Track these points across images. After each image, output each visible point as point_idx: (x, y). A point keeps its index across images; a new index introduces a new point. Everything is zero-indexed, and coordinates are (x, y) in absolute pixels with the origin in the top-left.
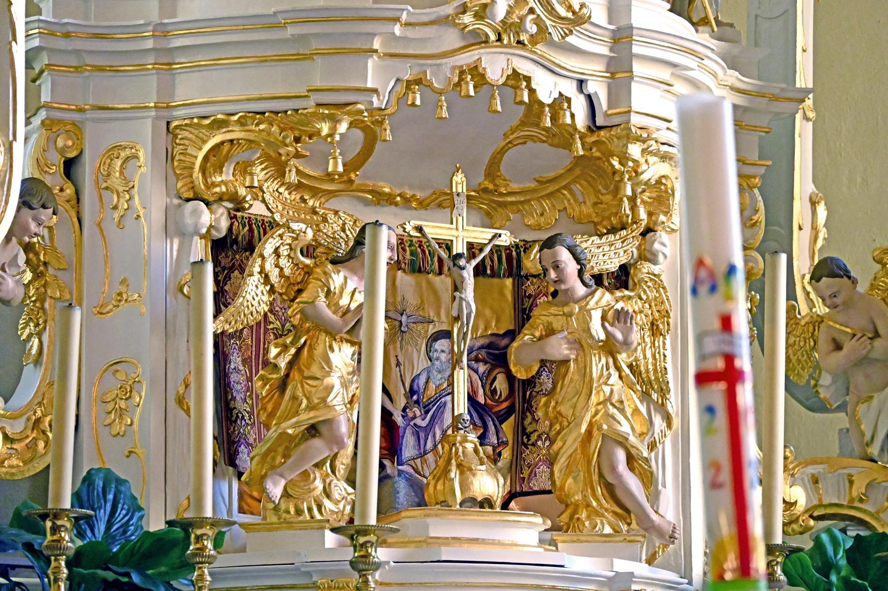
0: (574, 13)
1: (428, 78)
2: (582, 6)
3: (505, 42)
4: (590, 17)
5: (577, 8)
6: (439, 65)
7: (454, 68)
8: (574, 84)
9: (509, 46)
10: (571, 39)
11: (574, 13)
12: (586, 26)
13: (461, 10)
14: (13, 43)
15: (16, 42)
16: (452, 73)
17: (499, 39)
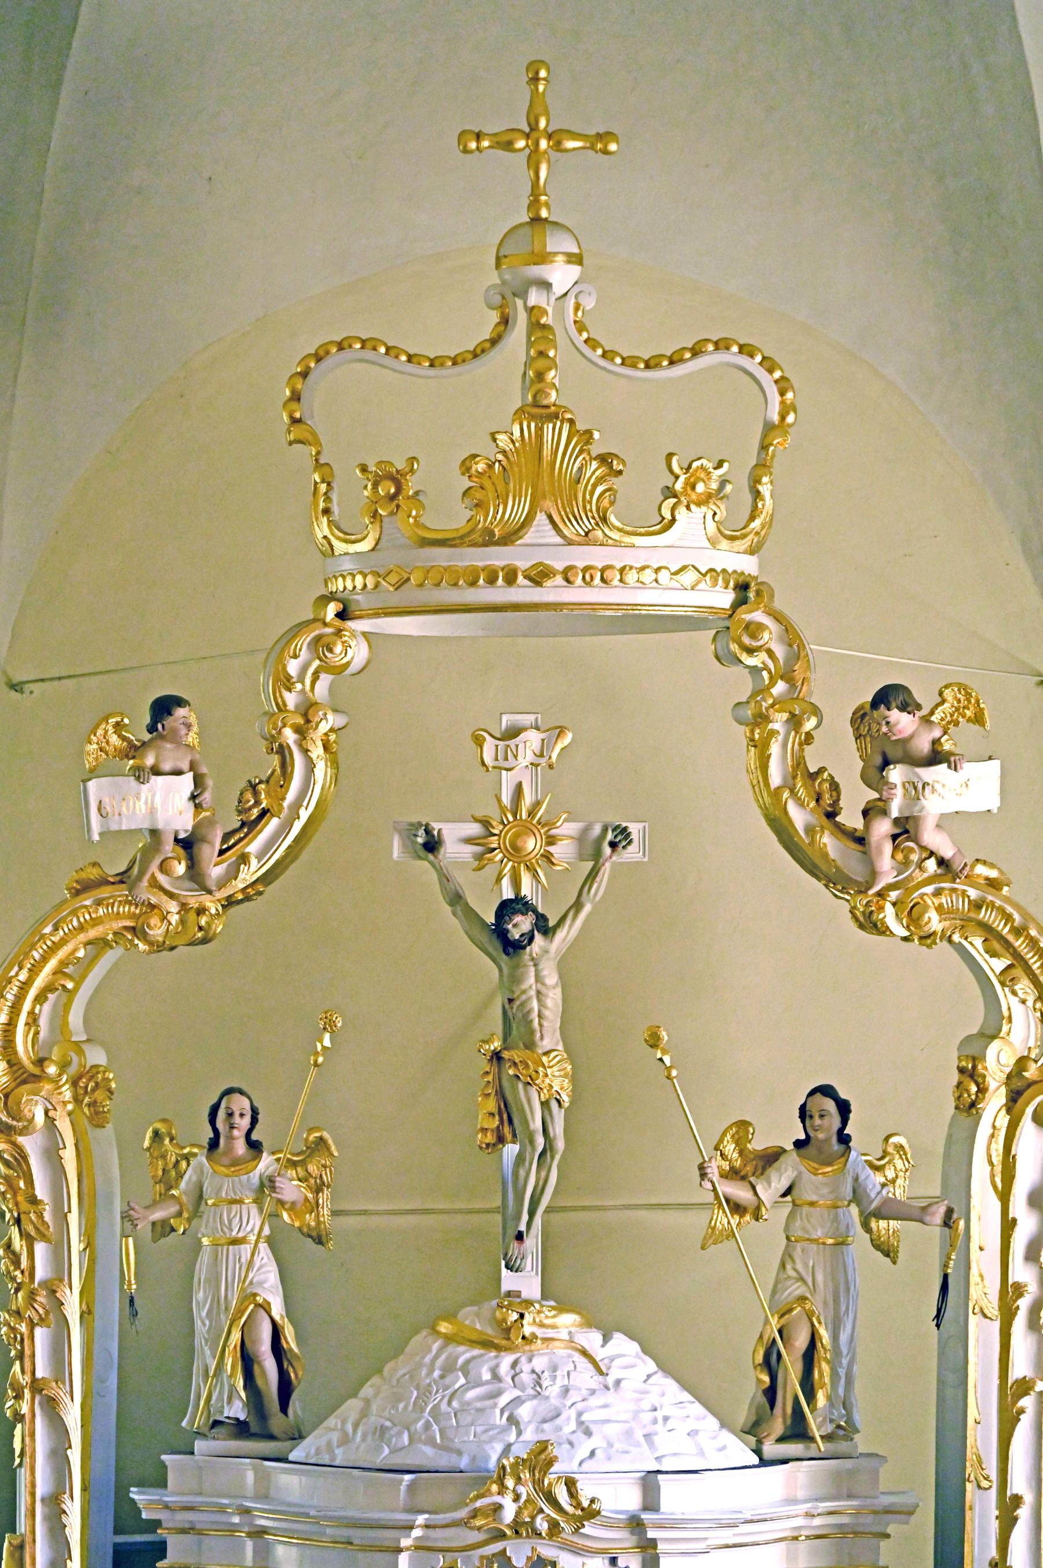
0: (583, 1509)
1: (459, 1566)
2: (592, 1501)
3: (524, 1534)
4: (599, 1512)
5: (585, 1504)
6: (468, 1557)
7: (482, 1557)
8: (607, 1562)
9: (528, 1536)
10: (588, 1529)
11: (583, 1509)
12: (598, 1518)
13: (472, 1514)
14: (68, 1561)
15: (71, 1560)
16: (482, 1563)
17: (517, 1532)
